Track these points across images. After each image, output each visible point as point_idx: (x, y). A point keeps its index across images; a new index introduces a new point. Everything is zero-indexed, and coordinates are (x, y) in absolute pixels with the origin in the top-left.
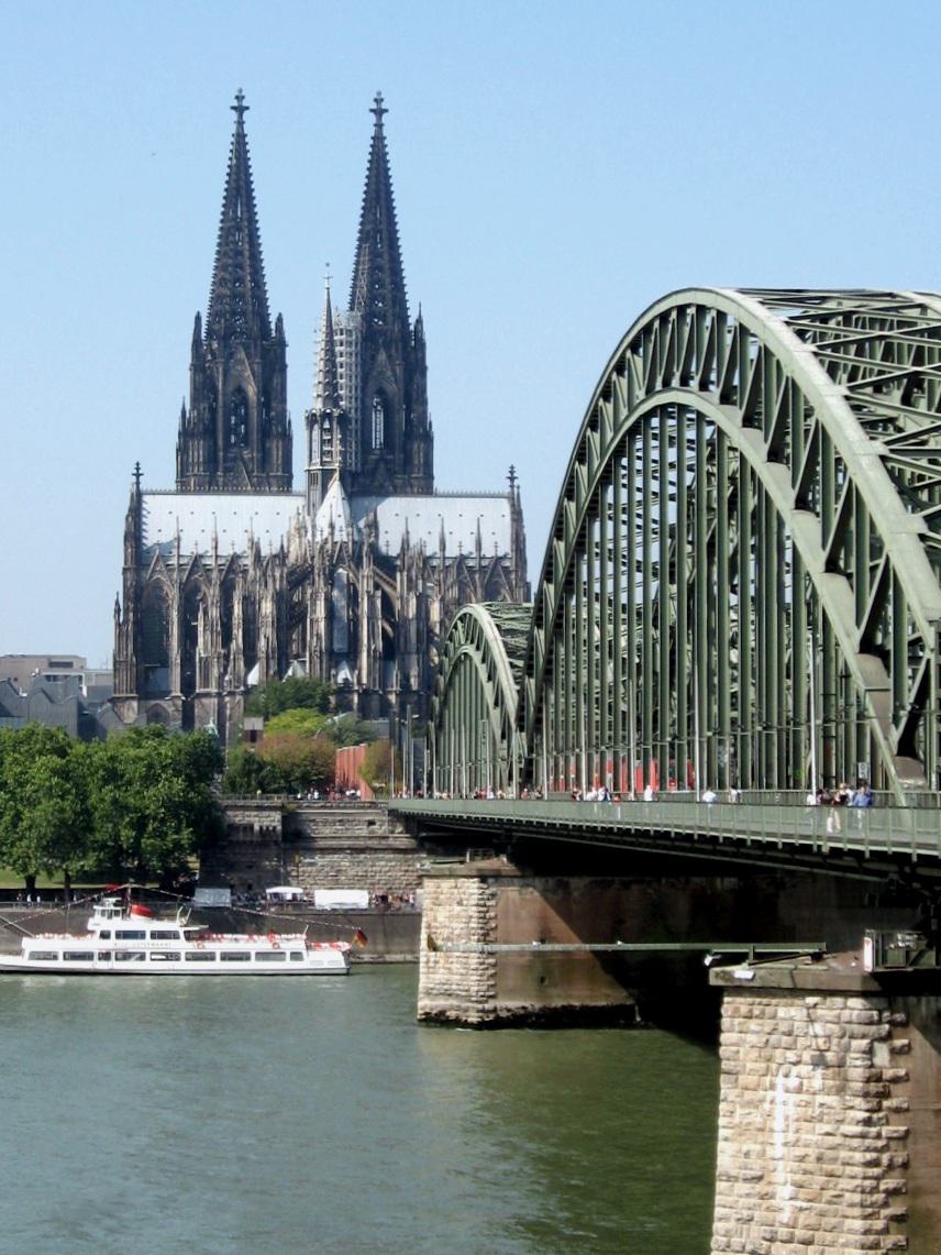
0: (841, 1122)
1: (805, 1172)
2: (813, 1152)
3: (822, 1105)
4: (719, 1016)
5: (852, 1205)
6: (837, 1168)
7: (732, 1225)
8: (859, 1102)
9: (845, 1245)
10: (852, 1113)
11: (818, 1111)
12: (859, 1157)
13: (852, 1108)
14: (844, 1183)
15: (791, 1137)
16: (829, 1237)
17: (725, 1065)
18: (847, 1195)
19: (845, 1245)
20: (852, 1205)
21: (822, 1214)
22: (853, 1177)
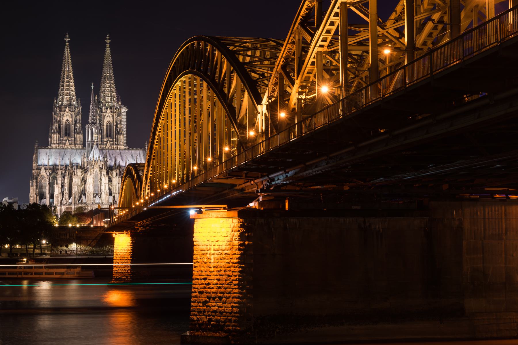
0: (231, 259)
1: (220, 275)
2: (223, 269)
3: (226, 254)
4: (194, 228)
5: (235, 285)
6: (230, 273)
7: (197, 294)
8: (237, 252)
9: (233, 298)
10: (235, 255)
11: (224, 256)
12: (237, 269)
13: (235, 254)
14: (233, 278)
15: (216, 264)
16: (228, 295)
17: (195, 243)
18: (234, 282)
19: (233, 298)
20: (235, 285)
21: (225, 288)
22: (236, 276)
